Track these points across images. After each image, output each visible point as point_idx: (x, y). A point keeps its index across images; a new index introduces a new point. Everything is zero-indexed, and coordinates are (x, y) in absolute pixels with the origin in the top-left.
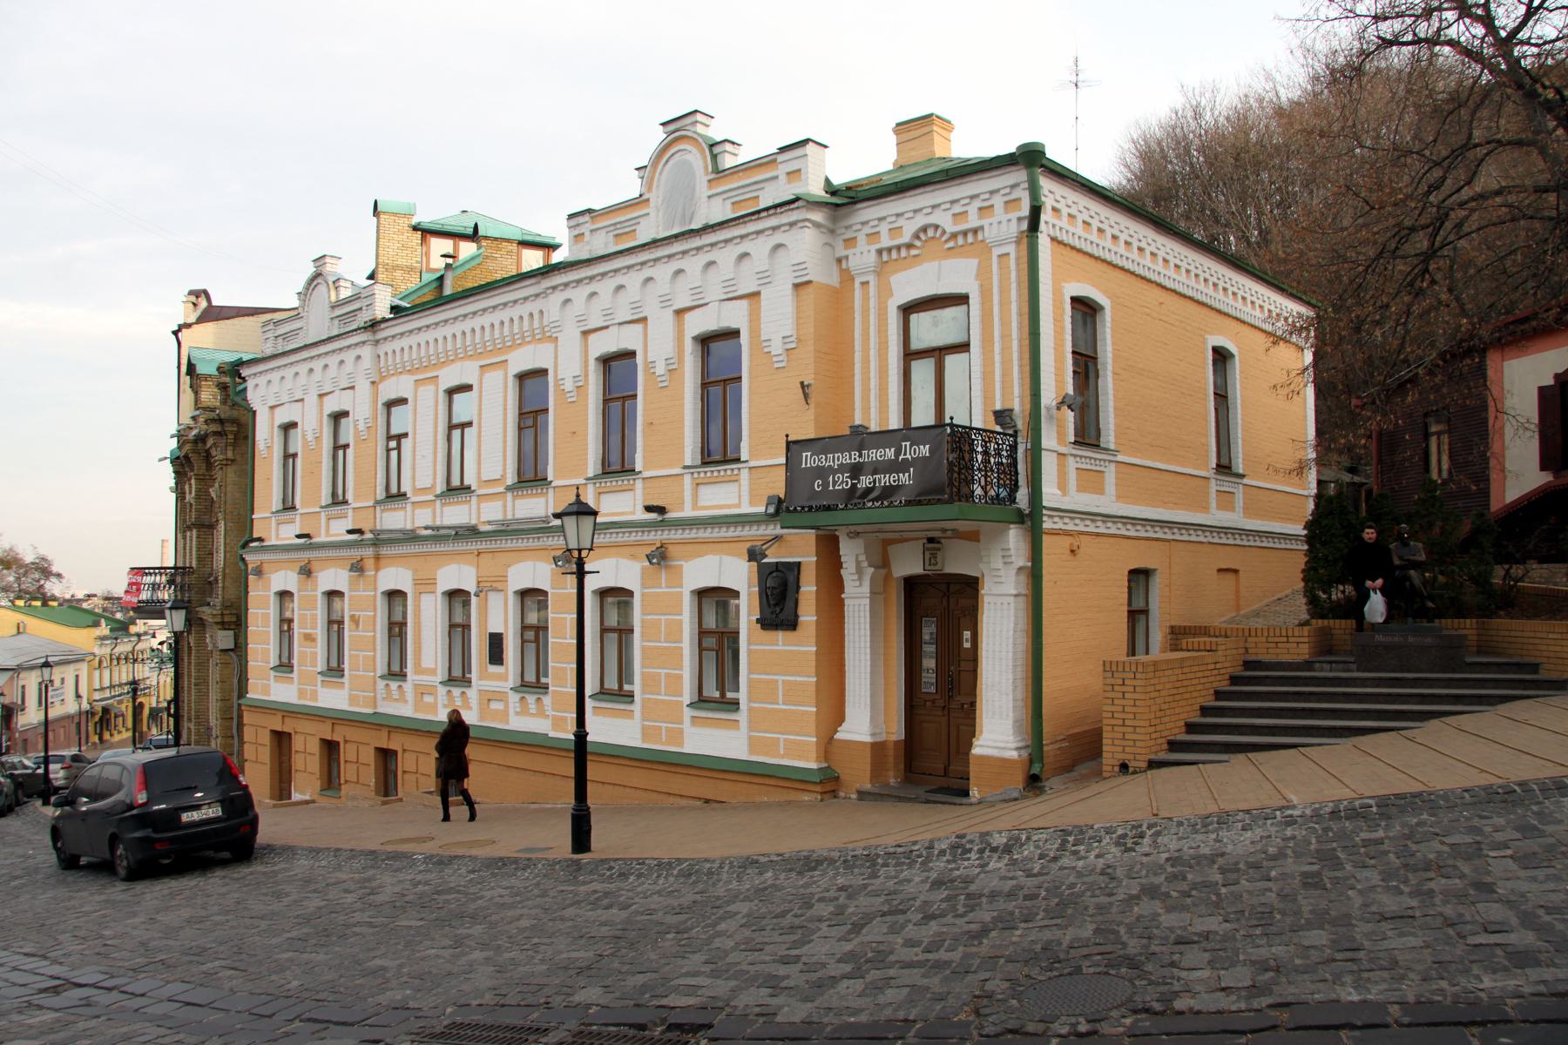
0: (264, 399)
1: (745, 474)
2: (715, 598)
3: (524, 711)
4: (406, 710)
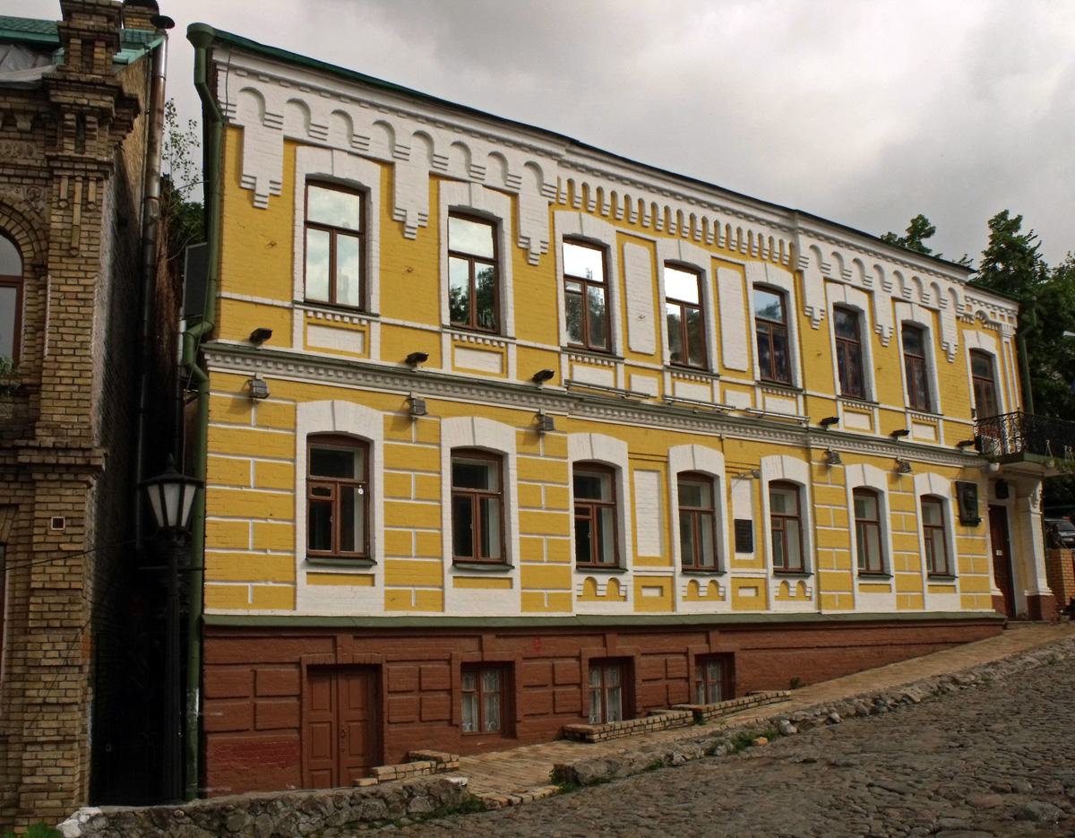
0: (270, 120)
1: (941, 422)
2: (931, 501)
3: (784, 596)
4: (623, 609)
